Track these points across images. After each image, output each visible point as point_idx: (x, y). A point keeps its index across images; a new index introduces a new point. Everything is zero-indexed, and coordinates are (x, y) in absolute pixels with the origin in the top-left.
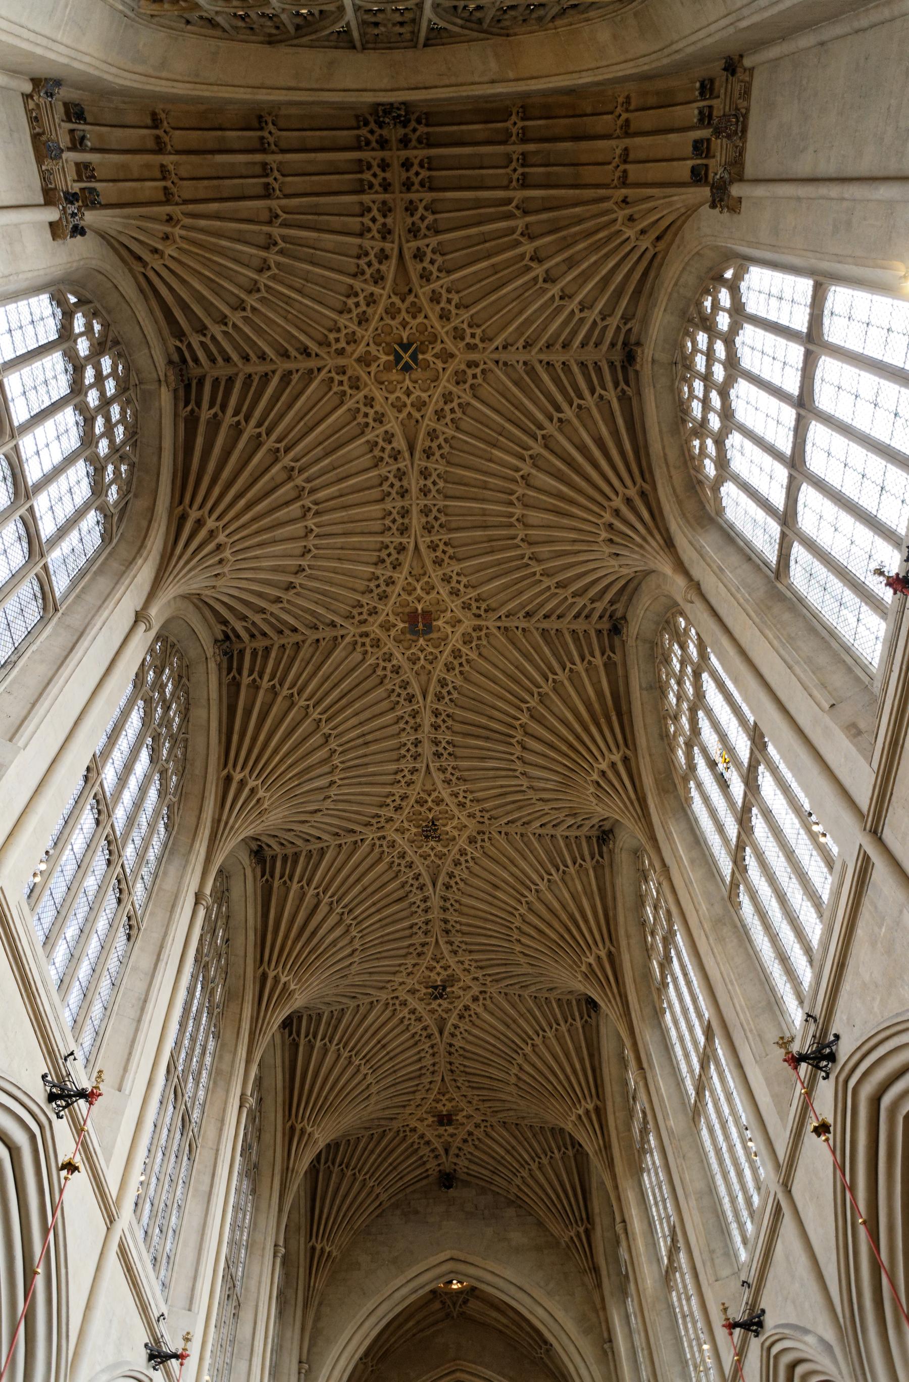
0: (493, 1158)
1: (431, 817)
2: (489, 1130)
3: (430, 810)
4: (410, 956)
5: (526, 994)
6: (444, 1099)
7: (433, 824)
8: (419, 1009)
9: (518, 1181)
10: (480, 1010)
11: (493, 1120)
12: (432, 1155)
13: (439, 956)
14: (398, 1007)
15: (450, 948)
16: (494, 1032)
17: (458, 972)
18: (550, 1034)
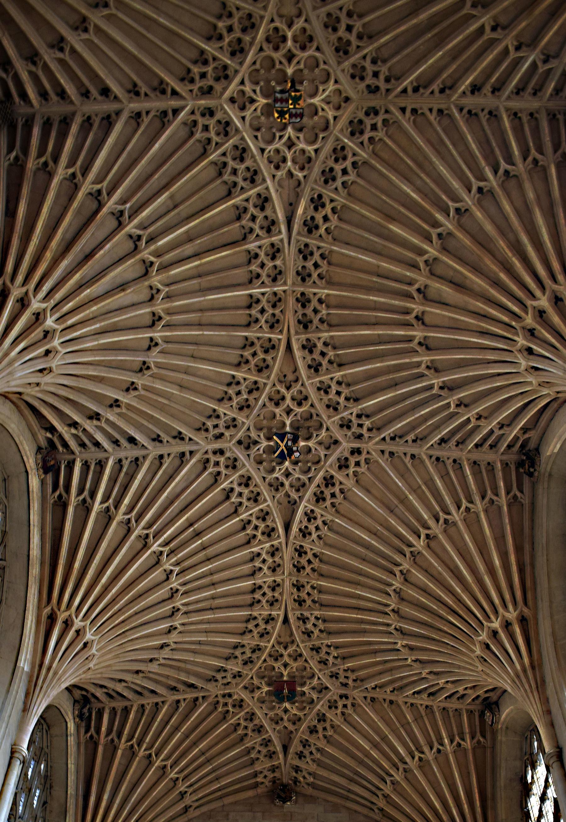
0: (353, 757)
1: (290, 71)
2: (350, 711)
3: (290, 57)
4: (245, 368)
5: (422, 451)
6: (285, 653)
7: (293, 82)
8: (257, 478)
9: (388, 789)
10: (349, 483)
11: (357, 694)
12: (264, 751)
13: (290, 377)
14: (222, 469)
15: (309, 358)
16: (368, 521)
17: (320, 408)
18: (456, 516)
